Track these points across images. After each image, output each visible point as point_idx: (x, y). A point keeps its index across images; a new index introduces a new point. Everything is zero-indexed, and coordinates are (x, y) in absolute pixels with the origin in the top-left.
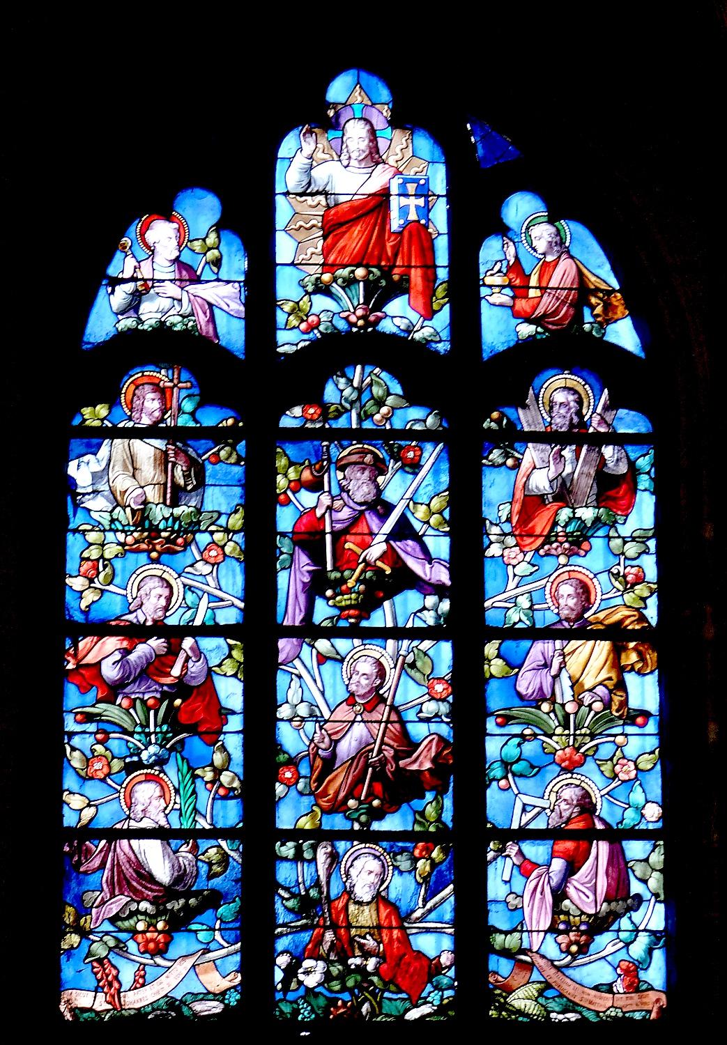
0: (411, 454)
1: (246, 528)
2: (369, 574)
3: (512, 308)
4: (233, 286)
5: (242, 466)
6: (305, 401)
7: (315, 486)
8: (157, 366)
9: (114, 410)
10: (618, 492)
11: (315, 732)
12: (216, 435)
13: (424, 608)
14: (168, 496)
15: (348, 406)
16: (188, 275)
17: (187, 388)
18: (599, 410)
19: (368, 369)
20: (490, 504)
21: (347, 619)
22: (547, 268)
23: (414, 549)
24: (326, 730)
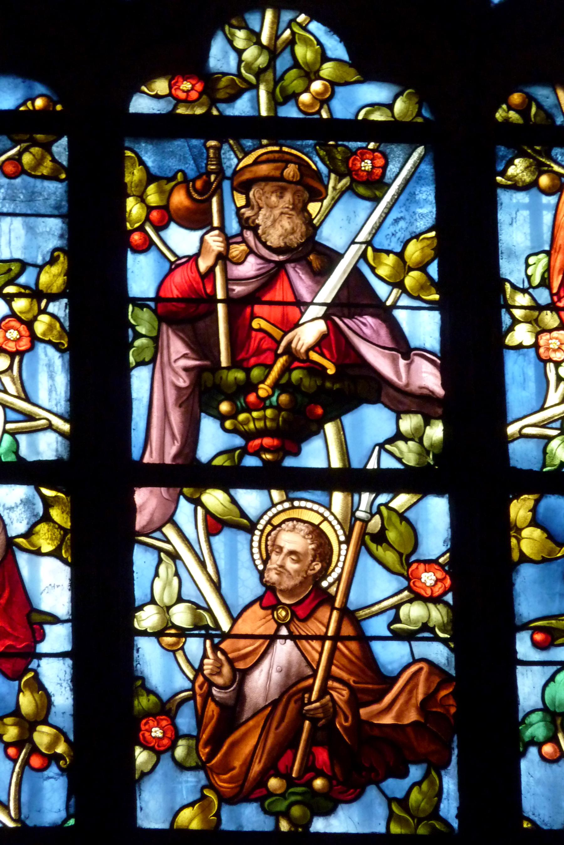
0: (367, 165)
1: (71, 291)
2: (296, 375)
5: (61, 181)
6: (173, 73)
7: (197, 219)
11: (205, 656)
13: (399, 436)
15: (251, 78)
19: (286, 16)
20: (512, 254)
21: (256, 454)
23: (377, 332)
24: (224, 653)
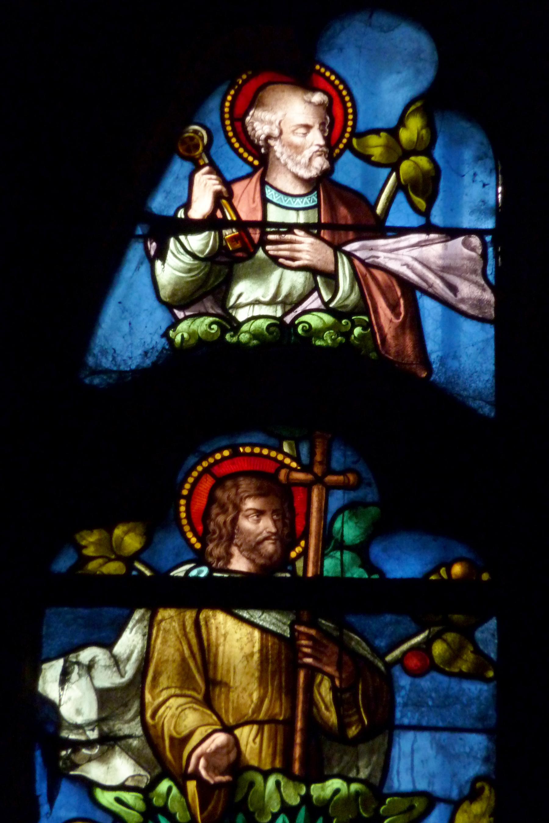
4: (465, 244)
8: (270, 434)
9: (158, 536)
12: (421, 602)
14: (298, 751)
16: (346, 214)
17: (345, 487)
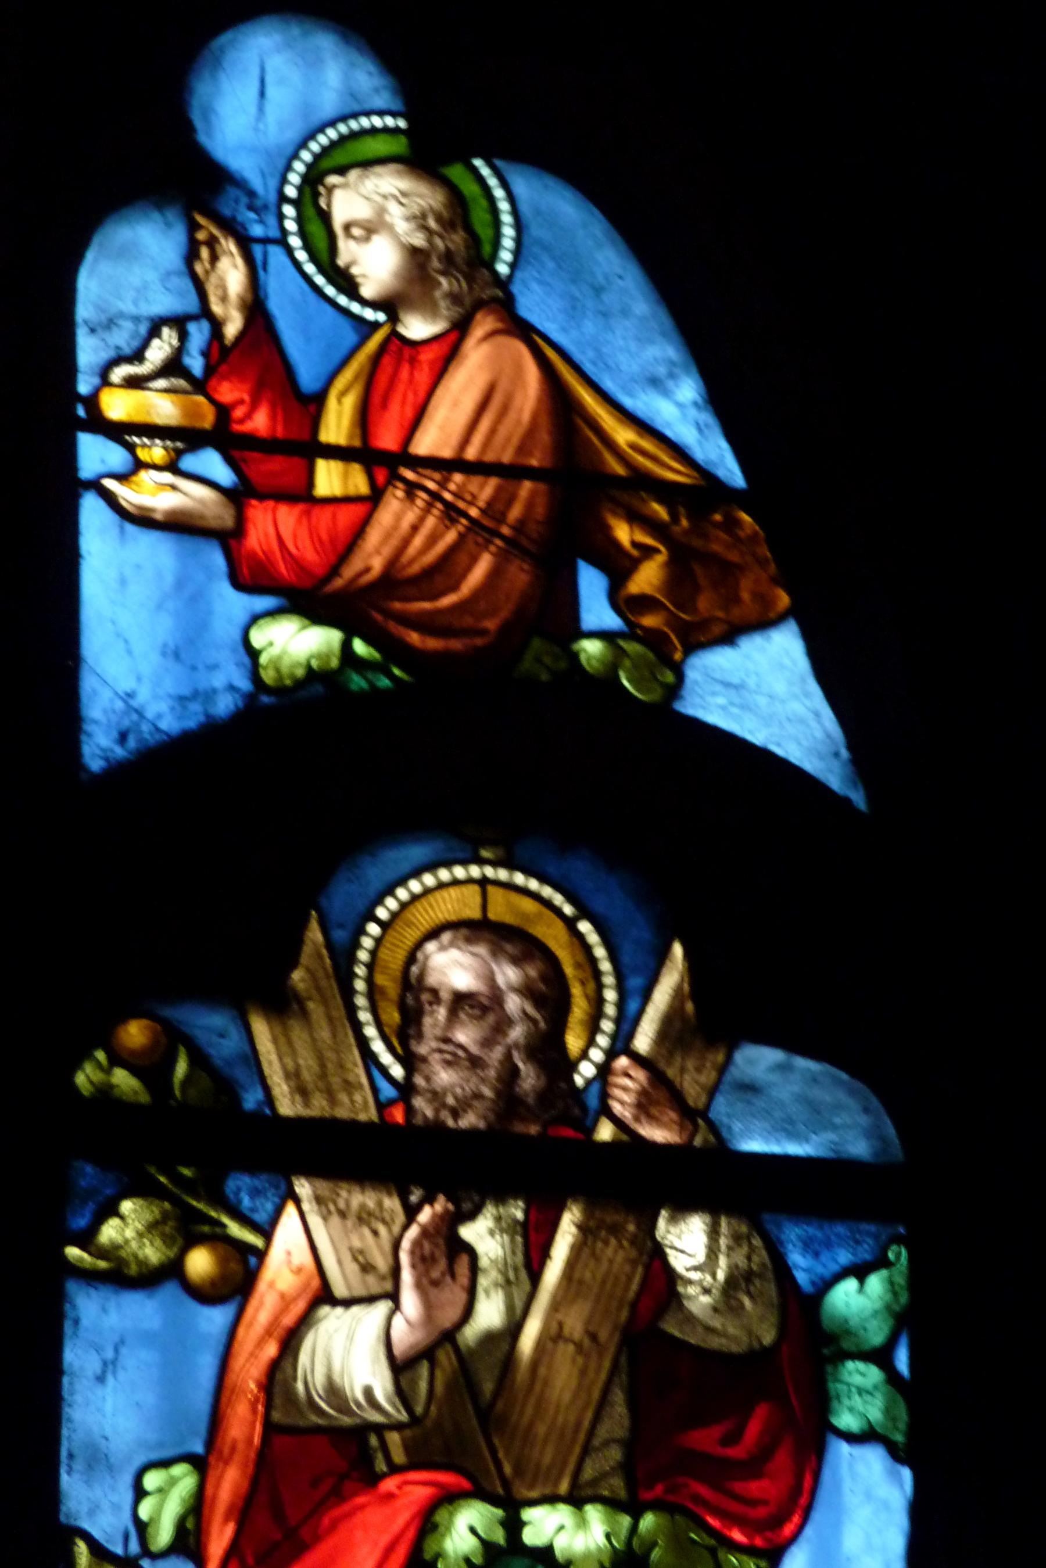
3: (229, 539)
10: (732, 1438)
18: (643, 1041)
20: (98, 1461)
22: (398, 372)
